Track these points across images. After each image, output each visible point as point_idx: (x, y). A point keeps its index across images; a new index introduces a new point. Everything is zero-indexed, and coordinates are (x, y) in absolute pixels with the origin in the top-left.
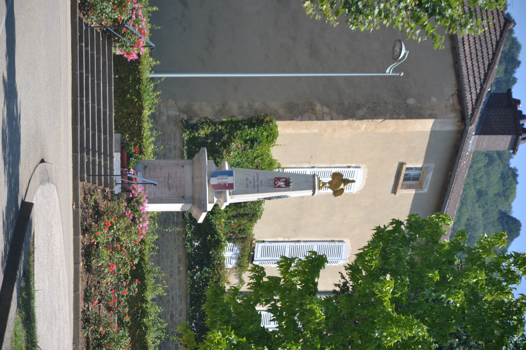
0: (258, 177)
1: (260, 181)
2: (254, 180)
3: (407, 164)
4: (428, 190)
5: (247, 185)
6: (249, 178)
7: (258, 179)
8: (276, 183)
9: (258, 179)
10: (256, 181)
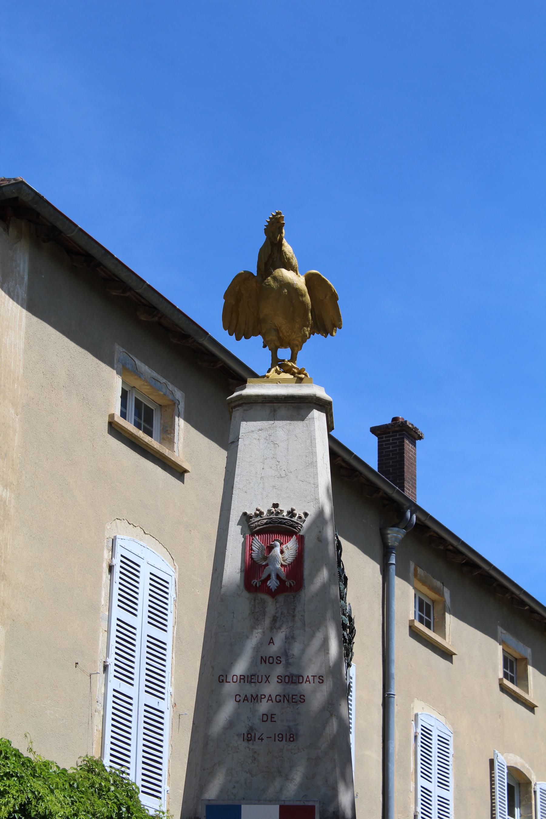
4: (180, 389)
5: (281, 737)
8: (273, 584)
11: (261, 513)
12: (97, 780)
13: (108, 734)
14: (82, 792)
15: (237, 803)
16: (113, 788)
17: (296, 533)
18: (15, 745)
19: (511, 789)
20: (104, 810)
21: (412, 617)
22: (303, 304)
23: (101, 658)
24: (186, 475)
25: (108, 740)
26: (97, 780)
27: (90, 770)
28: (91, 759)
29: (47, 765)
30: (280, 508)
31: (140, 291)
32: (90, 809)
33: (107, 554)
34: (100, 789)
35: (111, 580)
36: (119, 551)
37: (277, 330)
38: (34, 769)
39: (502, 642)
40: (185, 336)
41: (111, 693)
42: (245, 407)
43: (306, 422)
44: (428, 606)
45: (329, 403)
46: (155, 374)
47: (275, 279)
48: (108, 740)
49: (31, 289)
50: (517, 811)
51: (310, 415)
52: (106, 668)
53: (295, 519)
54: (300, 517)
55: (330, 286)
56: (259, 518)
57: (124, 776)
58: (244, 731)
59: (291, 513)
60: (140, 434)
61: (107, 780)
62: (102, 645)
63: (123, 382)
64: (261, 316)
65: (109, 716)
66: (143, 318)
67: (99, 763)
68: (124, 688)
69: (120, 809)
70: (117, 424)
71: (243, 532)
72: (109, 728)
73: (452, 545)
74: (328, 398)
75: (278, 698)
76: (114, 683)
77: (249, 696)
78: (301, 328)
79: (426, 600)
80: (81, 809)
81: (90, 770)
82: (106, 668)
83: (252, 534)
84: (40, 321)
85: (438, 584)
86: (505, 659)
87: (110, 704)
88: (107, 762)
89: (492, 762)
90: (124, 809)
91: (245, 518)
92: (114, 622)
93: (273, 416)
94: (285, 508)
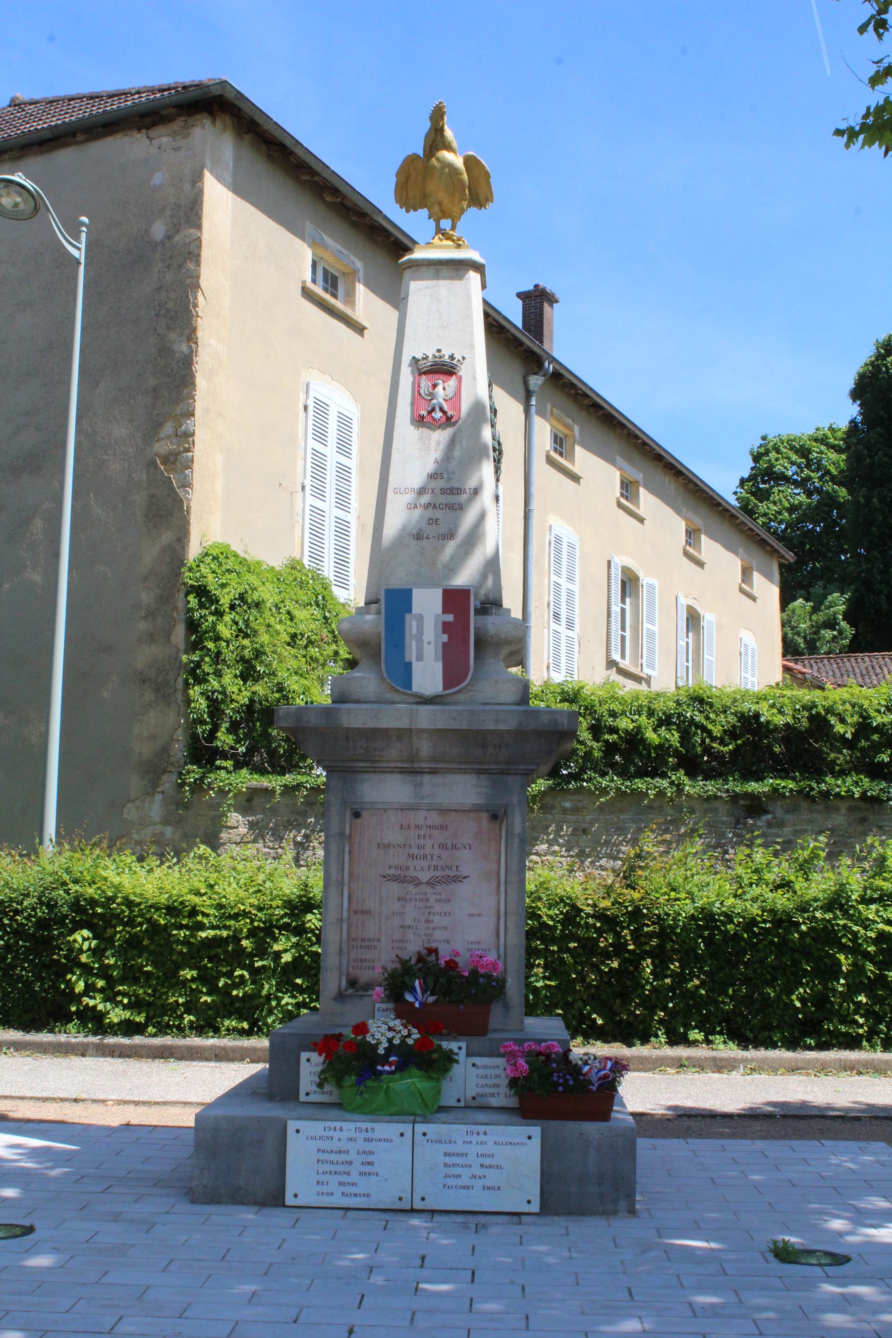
12: (299, 575)
14: (286, 584)
16: (311, 582)
20: (305, 598)
21: (548, 448)
25: (307, 544)
31: (325, 176)
32: (294, 597)
33: (302, 396)
34: (302, 582)
41: (308, 508)
48: (307, 544)
52: (303, 488)
57: (320, 572)
61: (306, 575)
62: (300, 469)
65: (307, 526)
67: (300, 562)
69: (317, 598)
70: (309, 289)
76: (310, 500)
79: (560, 435)
80: (287, 597)
87: (307, 517)
88: (306, 561)
92: (309, 451)
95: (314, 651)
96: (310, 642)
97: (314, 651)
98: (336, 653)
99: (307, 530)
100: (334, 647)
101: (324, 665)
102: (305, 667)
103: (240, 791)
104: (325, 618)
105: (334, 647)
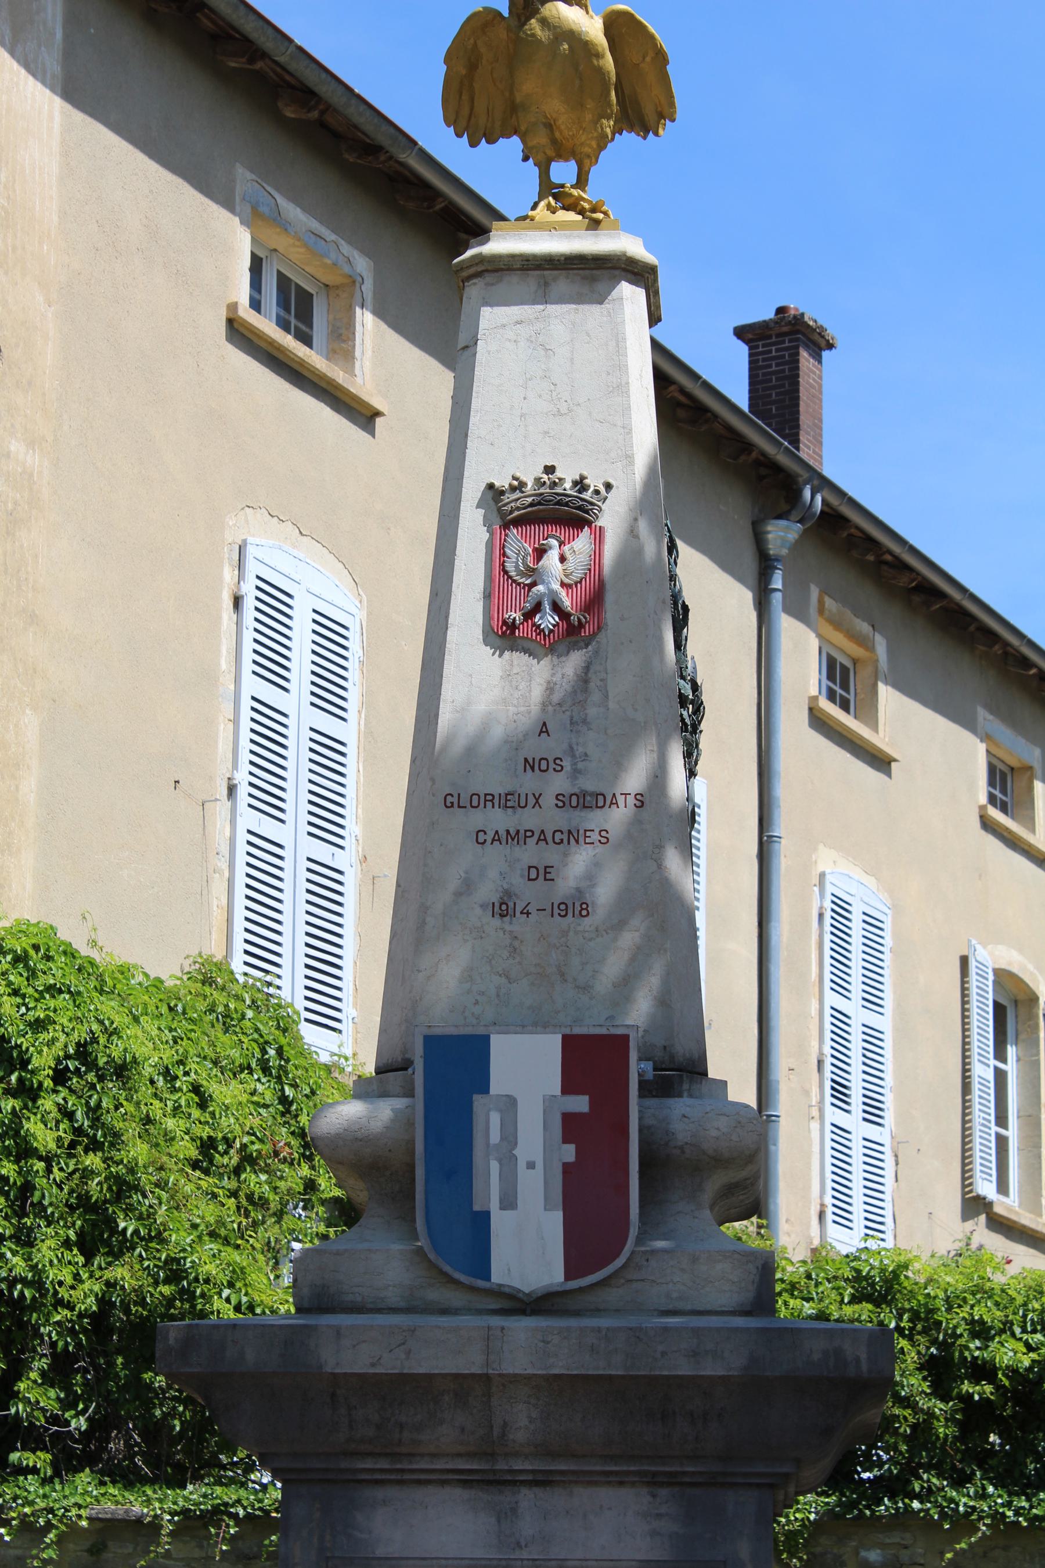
0: (489, 799)
1: (529, 783)
2: (516, 837)
3: (233, 299)
4: (363, 251)
6: (487, 891)
7: (509, 801)
9: (509, 801)
10: (528, 819)
11: (522, 484)
12: (220, 998)
13: (240, 913)
14: (192, 1020)
15: (481, 1031)
16: (250, 1014)
17: (589, 523)
18: (63, 935)
19: (999, 1010)
20: (235, 1053)
22: (600, 71)
23: (223, 771)
24: (379, 421)
26: (220, 998)
27: (208, 981)
28: (208, 961)
29: (124, 971)
30: (559, 473)
31: (281, 59)
32: (209, 1052)
33: (229, 575)
34: (227, 1016)
35: (239, 624)
36: (252, 568)
37: (550, 126)
38: (100, 978)
39: (986, 738)
40: (373, 149)
41: (242, 837)
42: (489, 278)
43: (606, 306)
44: (845, 670)
45: (653, 270)
46: (315, 225)
47: (544, 22)
48: (240, 924)
49: (68, 55)
50: (1011, 1051)
51: (615, 293)
52: (232, 790)
53: (587, 495)
54: (597, 492)
55: (652, 37)
56: (517, 494)
57: (271, 990)
58: (495, 898)
59: (580, 484)
60: (288, 341)
61: (238, 998)
62: (224, 746)
63: (254, 240)
64: (518, 100)
66: (289, 113)
67: (223, 967)
68: (268, 828)
69: (264, 1052)
70: (245, 324)
71: (487, 522)
72: (240, 903)
73: (890, 552)
74: (650, 258)
75: (558, 836)
76: (249, 819)
77: (503, 834)
78: (596, 121)
80: (192, 1051)
81: (208, 981)
82: (232, 790)
83: (506, 526)
84: (89, 120)
85: (864, 627)
86: (992, 770)
87: (241, 859)
88: (237, 966)
89: (964, 961)
90: (272, 1052)
91: (490, 494)
93: (543, 297)
94: (567, 475)
95: (255, 1181)
96: (248, 1160)
97: (255, 1181)
98: (310, 1185)
99: (241, 891)
100: (305, 1171)
101: (279, 1215)
102: (234, 1221)
103: (73, 1527)
104: (284, 1100)
105: (305, 1171)
